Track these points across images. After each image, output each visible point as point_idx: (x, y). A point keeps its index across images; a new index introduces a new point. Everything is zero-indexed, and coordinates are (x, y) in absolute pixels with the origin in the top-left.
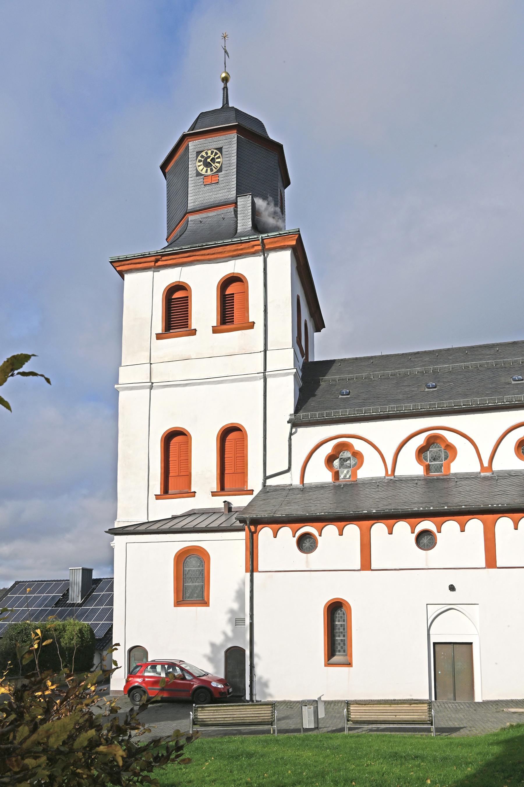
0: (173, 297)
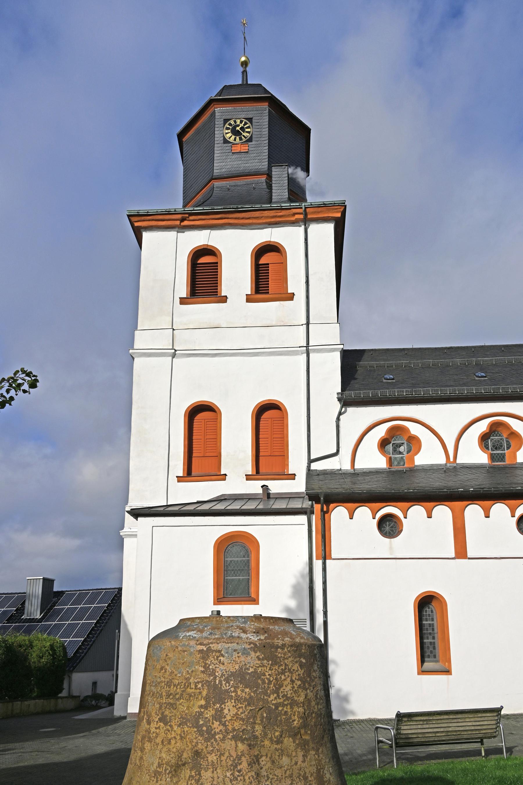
0: (198, 262)
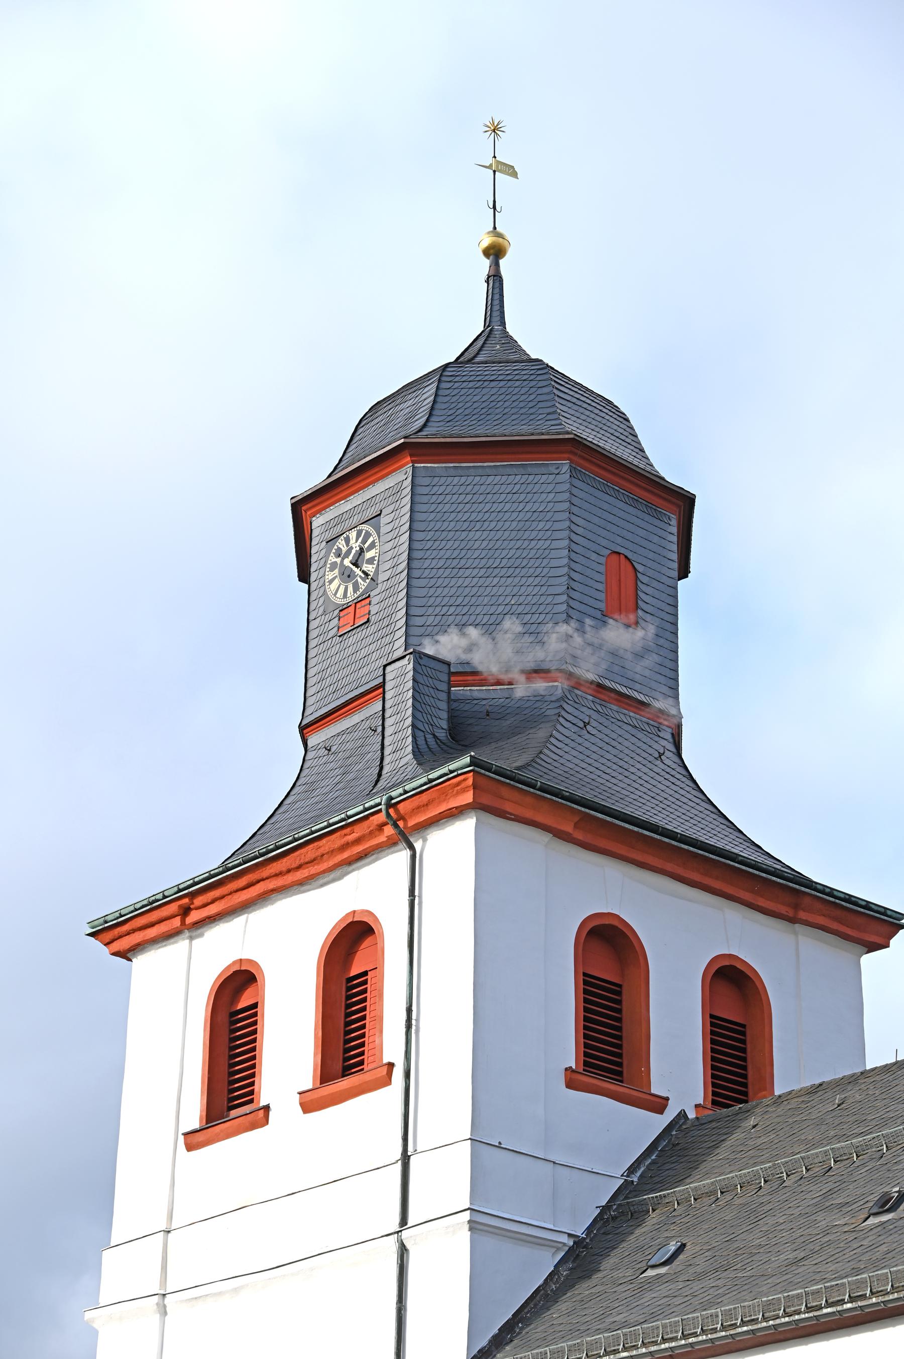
0: (240, 1006)
